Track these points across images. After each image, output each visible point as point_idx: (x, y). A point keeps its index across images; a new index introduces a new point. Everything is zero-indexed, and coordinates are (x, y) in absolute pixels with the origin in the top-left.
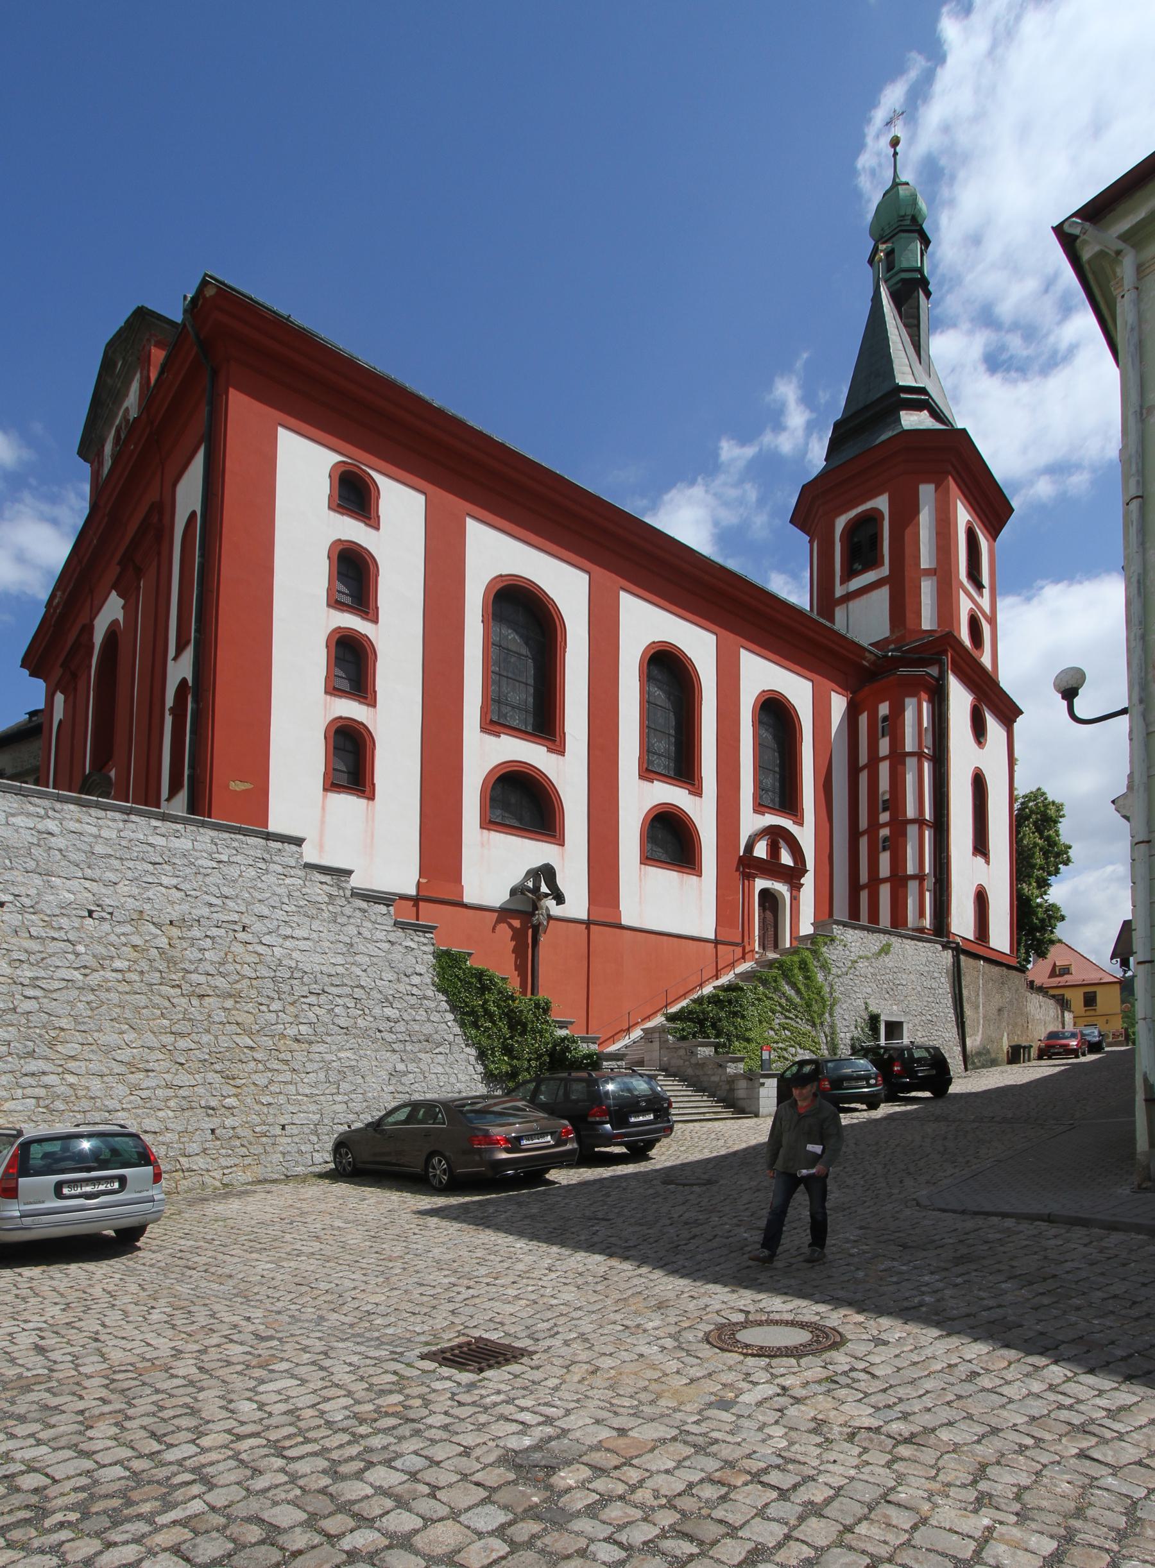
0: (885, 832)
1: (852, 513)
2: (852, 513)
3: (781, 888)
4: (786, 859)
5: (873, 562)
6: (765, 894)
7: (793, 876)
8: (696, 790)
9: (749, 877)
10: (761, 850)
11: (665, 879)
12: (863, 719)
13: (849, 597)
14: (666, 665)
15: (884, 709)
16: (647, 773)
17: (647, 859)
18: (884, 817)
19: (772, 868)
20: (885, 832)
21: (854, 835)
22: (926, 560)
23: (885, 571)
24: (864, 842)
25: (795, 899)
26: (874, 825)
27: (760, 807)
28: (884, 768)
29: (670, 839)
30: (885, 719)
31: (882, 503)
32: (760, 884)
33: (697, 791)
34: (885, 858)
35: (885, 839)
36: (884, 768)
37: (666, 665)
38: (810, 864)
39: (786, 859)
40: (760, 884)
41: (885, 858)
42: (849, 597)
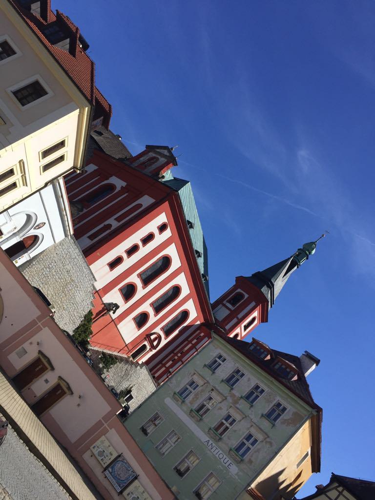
0: (176, 358)
1: (242, 292)
2: (242, 292)
3: (148, 347)
4: (155, 343)
5: (233, 305)
6: (145, 345)
7: (153, 347)
8: (155, 316)
9: (145, 339)
10: (153, 337)
11: (133, 325)
12: (199, 331)
13: (224, 305)
14: (177, 290)
15: (202, 334)
16: (152, 305)
17: (134, 319)
18: (179, 355)
19: (151, 342)
20: (176, 358)
21: (172, 351)
22: (240, 316)
23: (233, 308)
24: (172, 354)
25: (148, 352)
26: (176, 355)
27: (162, 329)
28: (190, 345)
29: (142, 320)
30: (200, 336)
31: (246, 296)
32: (146, 343)
33: (155, 316)
34: (171, 362)
35: (175, 359)
36: (190, 345)
37: (177, 290)
38: (158, 349)
39: (155, 343)
40: (146, 343)
41: (171, 362)
42: (224, 305)
